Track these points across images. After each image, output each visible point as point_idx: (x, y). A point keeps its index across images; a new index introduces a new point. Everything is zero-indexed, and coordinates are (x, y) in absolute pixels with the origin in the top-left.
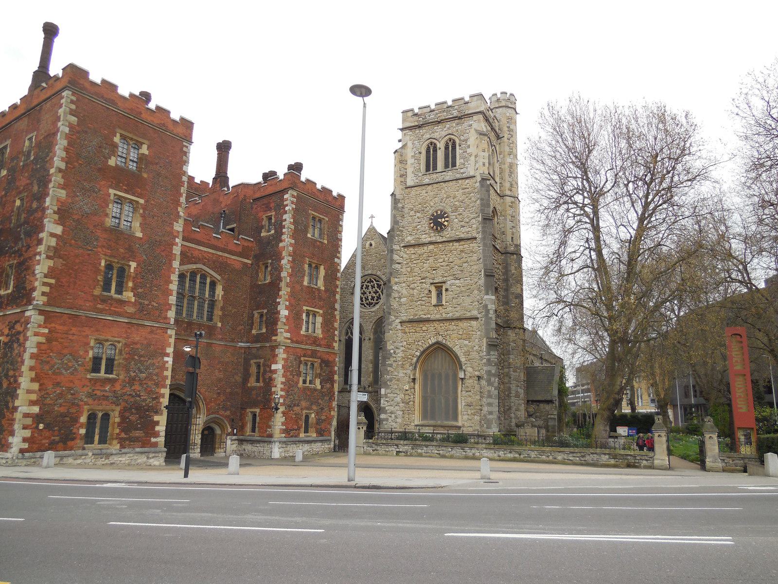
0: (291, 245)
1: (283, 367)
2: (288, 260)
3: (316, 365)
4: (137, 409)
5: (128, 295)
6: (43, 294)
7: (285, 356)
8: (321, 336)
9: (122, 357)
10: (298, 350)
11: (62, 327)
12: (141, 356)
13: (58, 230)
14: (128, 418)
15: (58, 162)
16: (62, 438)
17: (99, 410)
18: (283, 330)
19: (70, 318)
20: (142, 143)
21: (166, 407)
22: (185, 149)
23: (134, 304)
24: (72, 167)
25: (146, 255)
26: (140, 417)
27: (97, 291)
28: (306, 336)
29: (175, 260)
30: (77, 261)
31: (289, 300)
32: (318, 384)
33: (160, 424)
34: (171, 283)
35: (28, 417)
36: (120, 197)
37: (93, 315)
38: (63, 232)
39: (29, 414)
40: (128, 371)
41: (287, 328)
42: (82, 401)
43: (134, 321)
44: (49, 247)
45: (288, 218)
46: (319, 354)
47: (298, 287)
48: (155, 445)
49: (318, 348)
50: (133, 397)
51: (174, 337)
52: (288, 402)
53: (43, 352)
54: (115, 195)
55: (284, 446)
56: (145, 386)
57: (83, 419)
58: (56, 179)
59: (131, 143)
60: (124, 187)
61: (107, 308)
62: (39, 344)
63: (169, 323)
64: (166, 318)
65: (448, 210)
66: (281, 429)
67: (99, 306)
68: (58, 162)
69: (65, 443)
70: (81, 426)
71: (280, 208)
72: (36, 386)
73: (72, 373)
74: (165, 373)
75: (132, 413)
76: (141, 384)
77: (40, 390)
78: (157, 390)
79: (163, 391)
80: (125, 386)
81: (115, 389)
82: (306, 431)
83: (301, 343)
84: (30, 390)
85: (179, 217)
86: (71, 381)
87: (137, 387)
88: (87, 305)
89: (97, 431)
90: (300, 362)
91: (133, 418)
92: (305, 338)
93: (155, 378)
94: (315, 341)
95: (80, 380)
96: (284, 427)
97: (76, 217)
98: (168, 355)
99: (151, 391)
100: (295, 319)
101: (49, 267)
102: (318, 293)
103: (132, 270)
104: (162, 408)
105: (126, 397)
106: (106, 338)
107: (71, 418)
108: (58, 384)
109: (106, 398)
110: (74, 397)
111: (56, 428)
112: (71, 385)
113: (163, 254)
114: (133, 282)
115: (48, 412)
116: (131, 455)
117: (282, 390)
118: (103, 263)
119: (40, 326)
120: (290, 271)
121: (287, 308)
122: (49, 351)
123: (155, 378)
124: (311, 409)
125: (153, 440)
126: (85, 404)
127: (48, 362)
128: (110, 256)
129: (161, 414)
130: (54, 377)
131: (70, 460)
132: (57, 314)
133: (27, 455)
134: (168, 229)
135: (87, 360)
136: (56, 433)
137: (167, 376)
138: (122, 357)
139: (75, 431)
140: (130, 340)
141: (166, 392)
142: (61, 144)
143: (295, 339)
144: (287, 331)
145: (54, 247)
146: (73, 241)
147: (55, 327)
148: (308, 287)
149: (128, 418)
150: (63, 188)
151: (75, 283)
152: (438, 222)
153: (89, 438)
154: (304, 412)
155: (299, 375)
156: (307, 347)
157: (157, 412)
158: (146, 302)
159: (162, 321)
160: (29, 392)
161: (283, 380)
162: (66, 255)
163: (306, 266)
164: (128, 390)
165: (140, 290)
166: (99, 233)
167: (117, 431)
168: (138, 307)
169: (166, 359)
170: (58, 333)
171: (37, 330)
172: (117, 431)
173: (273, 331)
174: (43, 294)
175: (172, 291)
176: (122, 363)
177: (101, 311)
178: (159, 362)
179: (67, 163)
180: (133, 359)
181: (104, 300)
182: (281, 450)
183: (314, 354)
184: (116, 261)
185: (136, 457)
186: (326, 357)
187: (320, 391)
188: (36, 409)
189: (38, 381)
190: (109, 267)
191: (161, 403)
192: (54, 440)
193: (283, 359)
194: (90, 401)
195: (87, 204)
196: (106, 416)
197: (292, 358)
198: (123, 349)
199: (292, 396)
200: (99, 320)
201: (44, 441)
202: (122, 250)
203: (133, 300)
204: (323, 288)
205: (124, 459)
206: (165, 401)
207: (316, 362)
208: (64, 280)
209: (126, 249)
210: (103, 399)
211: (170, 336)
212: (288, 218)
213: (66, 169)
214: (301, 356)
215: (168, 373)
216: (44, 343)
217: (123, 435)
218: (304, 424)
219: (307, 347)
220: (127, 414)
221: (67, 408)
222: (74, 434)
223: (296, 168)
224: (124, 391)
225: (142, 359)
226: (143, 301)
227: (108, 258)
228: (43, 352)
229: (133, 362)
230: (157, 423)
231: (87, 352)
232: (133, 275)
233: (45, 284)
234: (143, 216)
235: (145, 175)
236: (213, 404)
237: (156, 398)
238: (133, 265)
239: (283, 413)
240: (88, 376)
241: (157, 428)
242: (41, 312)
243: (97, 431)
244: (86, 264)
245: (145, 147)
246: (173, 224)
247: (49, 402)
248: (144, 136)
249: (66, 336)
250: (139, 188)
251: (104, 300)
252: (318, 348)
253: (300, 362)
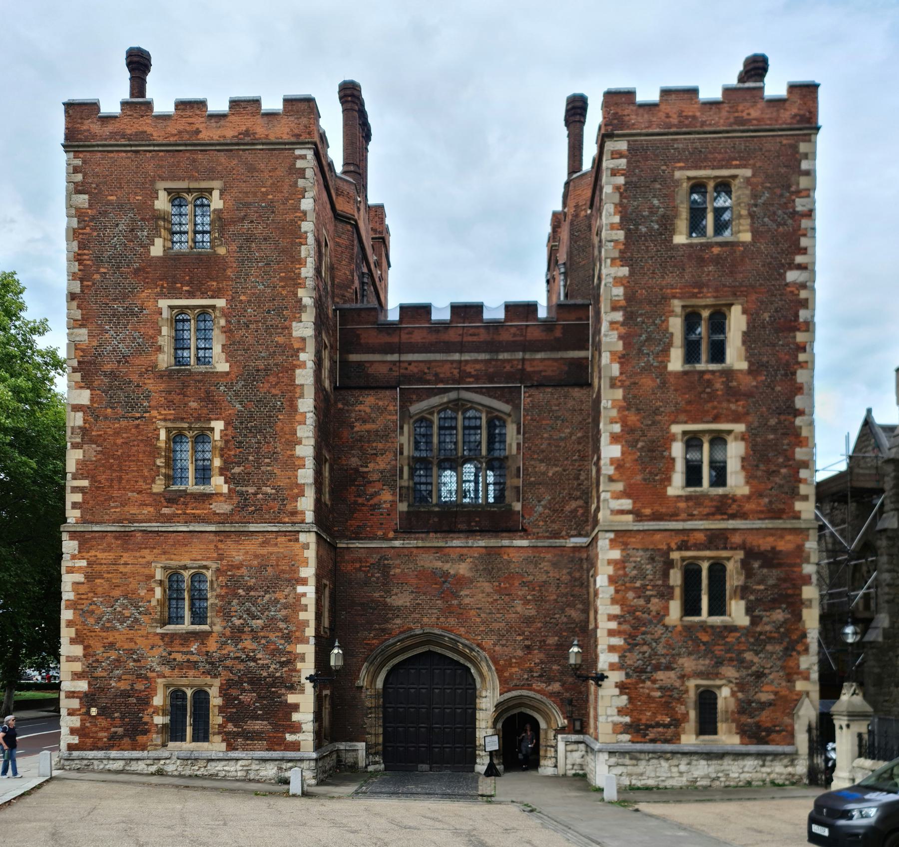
0: (618, 281)
1: (612, 580)
2: (612, 323)
3: (731, 566)
4: (251, 682)
6: (75, 505)
7: (616, 554)
8: (746, 490)
9: (215, 593)
10: (658, 537)
11: (106, 554)
12: (250, 589)
14: (236, 698)
16: (128, 730)
17: (187, 686)
18: (608, 495)
19: (116, 538)
20: (210, 191)
21: (310, 678)
22: (300, 164)
23: (229, 497)
24: (90, 283)
25: (241, 403)
26: (260, 698)
27: (158, 487)
28: (688, 498)
29: (302, 396)
30: (119, 441)
31: (624, 422)
32: (737, 613)
33: (301, 709)
34: (300, 443)
35: (73, 697)
36: (182, 309)
37: (154, 526)
38: (92, 400)
39: (74, 692)
40: (226, 614)
41: (619, 486)
42: (154, 671)
43: (227, 528)
44: (73, 428)
46: (737, 539)
47: (648, 383)
48: (296, 746)
49: (731, 524)
50: (242, 661)
51: (313, 546)
52: (633, 659)
53: (83, 597)
54: (171, 308)
55: (627, 761)
56: (263, 641)
57: (158, 700)
59: (190, 198)
60: (185, 288)
61: (180, 512)
62: (76, 584)
63: (303, 522)
64: (294, 513)
66: (615, 724)
67: (165, 511)
69: (133, 739)
70: (156, 711)
72: (78, 650)
73: (131, 627)
74: (302, 616)
75: (244, 691)
76: (255, 638)
77: (85, 656)
78: (289, 648)
79: (300, 648)
80: (225, 643)
81: (208, 649)
82: (707, 726)
83: (673, 516)
84: (71, 657)
85: (300, 307)
86: (131, 640)
87: (248, 644)
88: (145, 512)
89: (189, 720)
90: (670, 564)
91: (246, 698)
92: (682, 505)
93: (282, 625)
94: (724, 507)
95: (146, 637)
96: (627, 719)
97: (108, 368)
98: (304, 582)
99: (277, 649)
100: (648, 457)
101: (78, 462)
102: (726, 384)
103: (217, 436)
104: (303, 680)
105: (228, 663)
106: (182, 563)
107: (138, 699)
108: (111, 646)
109: (194, 665)
110: (138, 664)
111: (116, 715)
112: (132, 645)
113: (274, 391)
114: (222, 456)
115: (101, 689)
116: (246, 762)
117: (611, 633)
118: (163, 435)
119: (73, 557)
120: (619, 346)
121: (615, 439)
122: (92, 595)
123: (282, 625)
124: (717, 675)
125: (289, 737)
126: (159, 676)
127: (93, 612)
128: (174, 420)
129: (302, 691)
130: (104, 634)
131: (141, 766)
132: (97, 535)
133: (75, 754)
134: (280, 340)
135: (154, 603)
136: (118, 722)
137: (306, 623)
138: (215, 593)
139: (144, 720)
140: (225, 562)
141: (308, 650)
143: (648, 511)
144: (617, 496)
145: (80, 428)
146: (109, 410)
147: (96, 556)
148: (685, 373)
149: (236, 698)
150: (82, 326)
151: (120, 479)
153: (174, 732)
154: (692, 683)
155: (666, 594)
156: (689, 525)
157: (293, 687)
158: (251, 490)
159: (287, 520)
160: (70, 659)
161: (616, 610)
162: (101, 435)
163: (676, 325)
164: (230, 648)
165: (237, 470)
166: (151, 384)
167: (220, 720)
168: (235, 501)
169: (300, 589)
170: (101, 564)
171: (70, 564)
172: (220, 720)
174: (75, 505)
175: (303, 458)
176: (216, 605)
177: (169, 519)
178: (286, 597)
179: (82, 280)
180: (236, 595)
181: (172, 499)
182: (619, 770)
183: (717, 539)
184: (186, 425)
185: (254, 767)
186: (765, 544)
187: (746, 632)
188: (83, 686)
189: (81, 642)
190: (176, 437)
191: (299, 671)
192: (116, 732)
193: (610, 562)
194: (166, 670)
195: (123, 341)
196: (201, 697)
197: (639, 556)
198: (214, 579)
199: (645, 648)
200: (166, 534)
201: (102, 734)
202: (193, 405)
203: (225, 489)
204: (744, 365)
205: (235, 769)
206: (307, 668)
207: (728, 559)
208: (102, 478)
209: (201, 400)
210: (189, 668)
211: (306, 546)
213: (82, 291)
214: (670, 549)
215: (309, 615)
216: (83, 583)
217: (230, 727)
218: (692, 714)
219: (689, 525)
220: (234, 692)
221: (130, 682)
222: (146, 723)
224: (224, 652)
225: (252, 593)
226: (244, 489)
227: (169, 425)
228: (83, 597)
229: (235, 602)
230: (296, 707)
231: (152, 590)
232: (219, 444)
233: (75, 490)
234: (227, 331)
235: (222, 251)
236: (514, 670)
237: (288, 662)
238: (218, 426)
239: (622, 687)
240: (159, 631)
241: (295, 717)
242: (73, 535)
243: (189, 720)
244: (136, 443)
245: (216, 194)
246: (289, 328)
247: (102, 674)
248: (211, 175)
249: (115, 567)
250: (212, 279)
251: (172, 499)
252: (731, 524)
253: (670, 564)
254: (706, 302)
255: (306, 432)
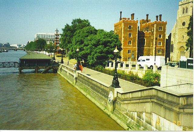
5: (131, 45)
13: (123, 39)
15: (123, 32)
45: (155, 29)
58: (123, 33)
65: (185, 22)
68: (123, 32)
71: (154, 26)
94: (160, 47)
142: (123, 29)
152: (184, 24)
173: (153, 46)
183: (160, 49)
212: (155, 29)
215: (137, 53)
223: (161, 16)
238: (132, 41)
251: (129, 45)
254: (160, 34)
255: (137, 42)
